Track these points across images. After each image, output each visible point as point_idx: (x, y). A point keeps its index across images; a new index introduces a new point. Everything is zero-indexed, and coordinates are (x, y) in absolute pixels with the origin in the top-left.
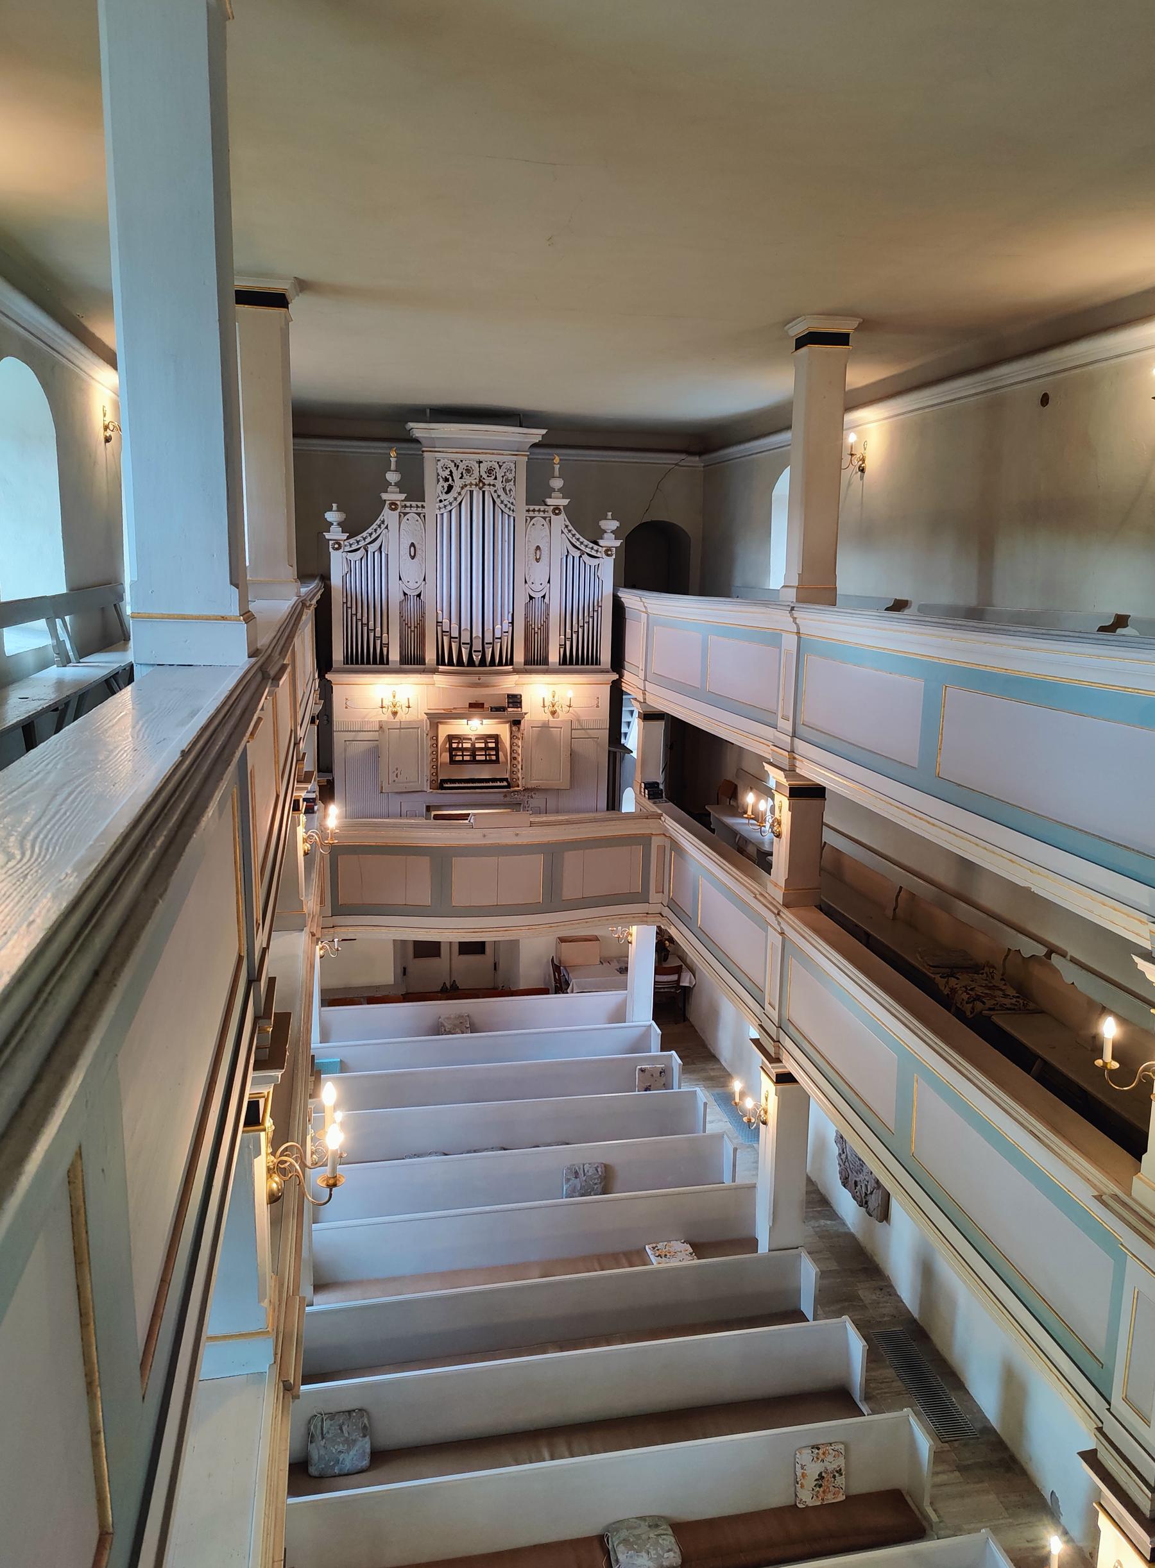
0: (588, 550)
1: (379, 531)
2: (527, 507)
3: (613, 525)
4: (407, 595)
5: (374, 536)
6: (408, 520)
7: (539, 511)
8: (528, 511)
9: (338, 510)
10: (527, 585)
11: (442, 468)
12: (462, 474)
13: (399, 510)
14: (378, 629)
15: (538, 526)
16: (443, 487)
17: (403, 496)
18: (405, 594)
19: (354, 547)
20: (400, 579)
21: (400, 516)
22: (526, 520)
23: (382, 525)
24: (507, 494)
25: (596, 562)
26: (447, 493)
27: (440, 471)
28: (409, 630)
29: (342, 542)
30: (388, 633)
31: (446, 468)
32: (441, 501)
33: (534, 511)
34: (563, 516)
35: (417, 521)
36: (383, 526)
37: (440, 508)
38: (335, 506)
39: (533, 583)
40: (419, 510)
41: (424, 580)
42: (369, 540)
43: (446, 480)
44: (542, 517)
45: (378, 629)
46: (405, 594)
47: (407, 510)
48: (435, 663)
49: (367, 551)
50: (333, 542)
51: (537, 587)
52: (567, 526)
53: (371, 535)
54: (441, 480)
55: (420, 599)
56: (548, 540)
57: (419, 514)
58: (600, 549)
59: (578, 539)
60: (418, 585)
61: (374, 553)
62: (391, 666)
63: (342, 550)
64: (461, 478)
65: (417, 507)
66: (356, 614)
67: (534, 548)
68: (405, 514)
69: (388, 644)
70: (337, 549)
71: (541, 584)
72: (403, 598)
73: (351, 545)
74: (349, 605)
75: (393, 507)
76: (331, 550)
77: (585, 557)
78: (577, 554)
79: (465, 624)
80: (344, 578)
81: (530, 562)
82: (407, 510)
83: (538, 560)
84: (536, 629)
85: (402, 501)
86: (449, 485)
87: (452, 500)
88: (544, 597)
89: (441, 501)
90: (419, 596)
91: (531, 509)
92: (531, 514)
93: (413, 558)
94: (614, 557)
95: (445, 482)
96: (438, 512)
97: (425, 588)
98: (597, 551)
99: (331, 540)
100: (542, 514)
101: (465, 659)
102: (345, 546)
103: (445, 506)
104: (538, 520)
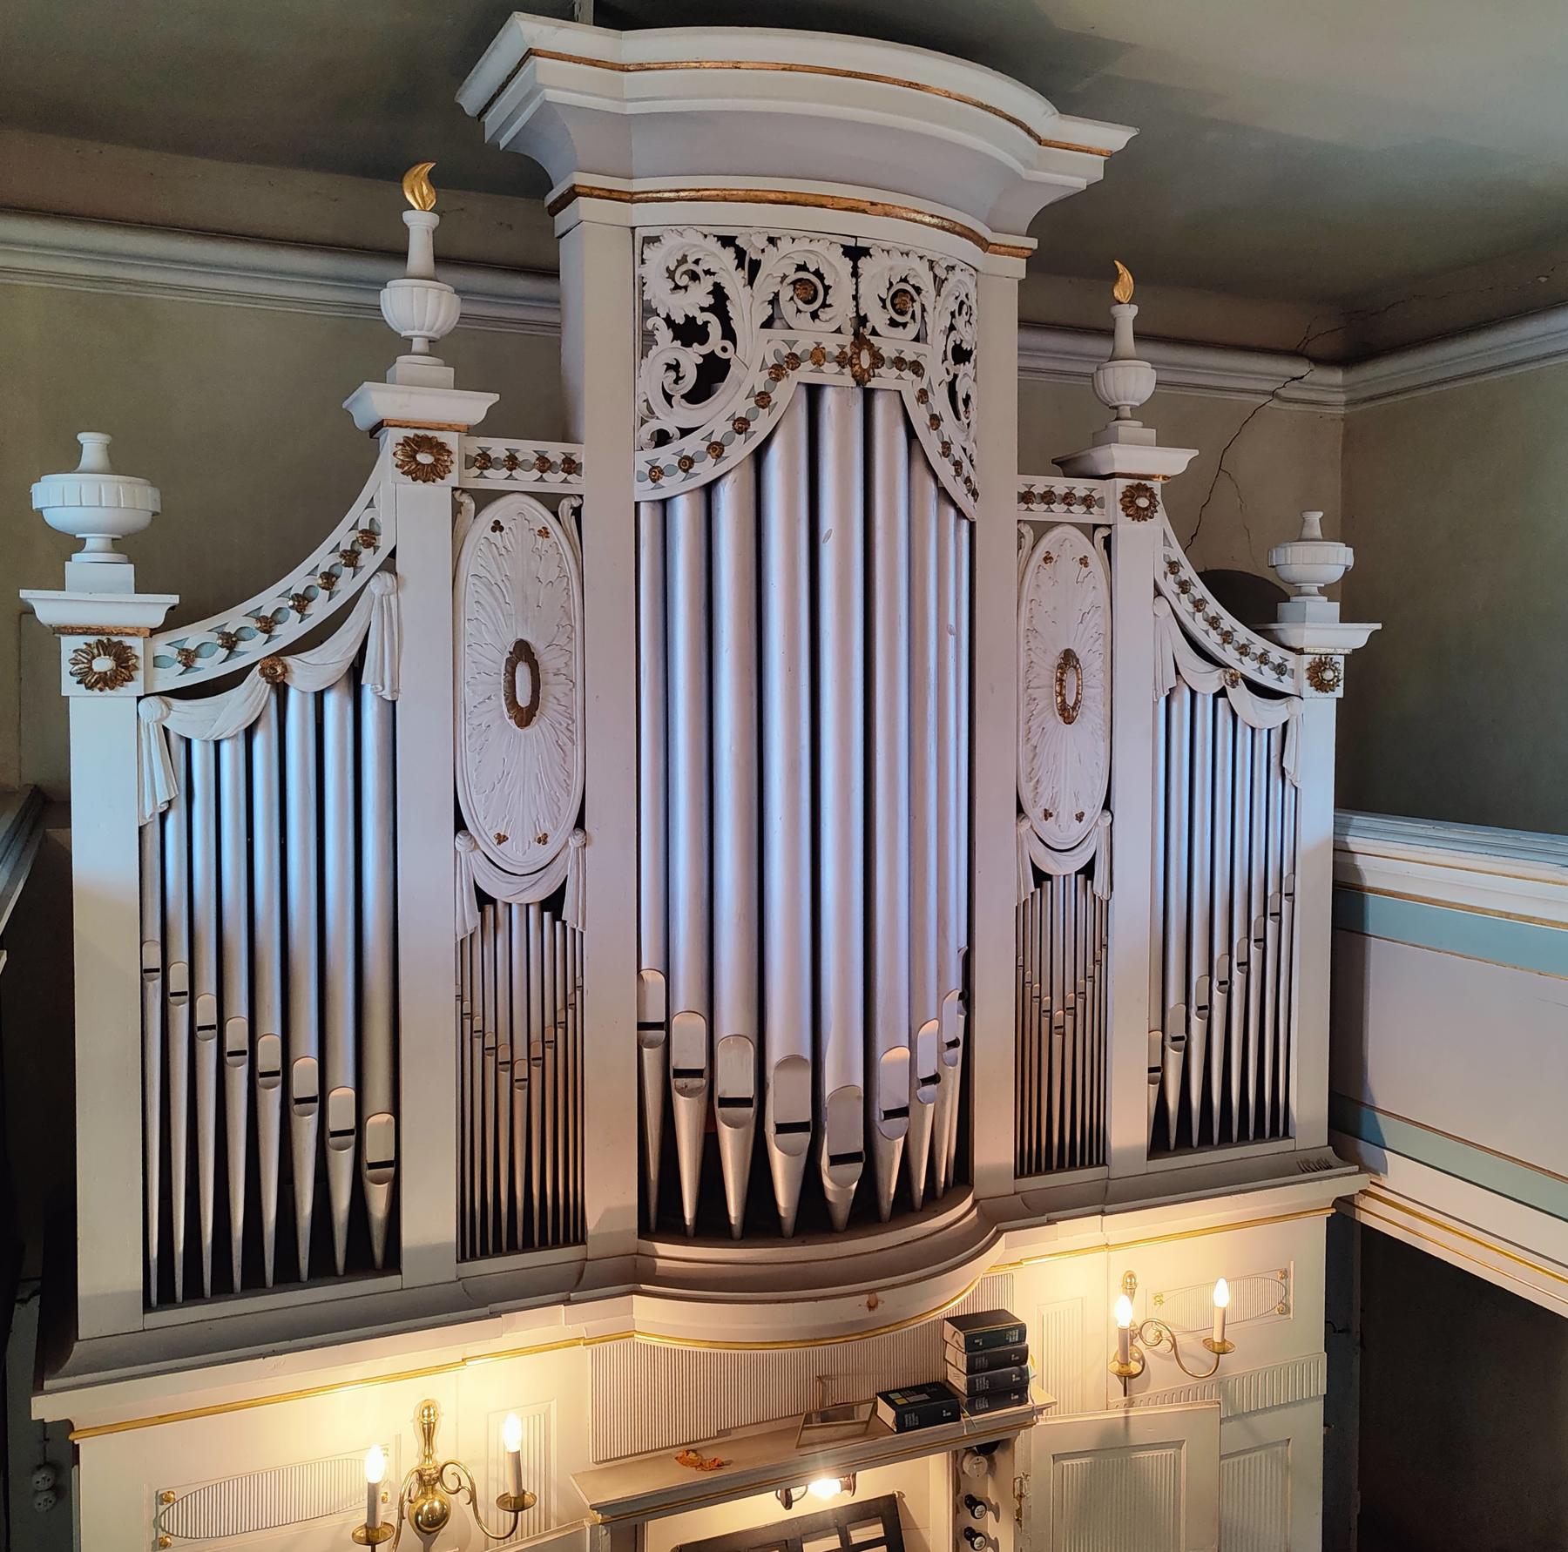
0: (1249, 668)
1: (346, 585)
2: (1021, 483)
3: (1335, 560)
4: (493, 901)
5: (321, 609)
6: (497, 527)
7: (1068, 499)
8: (1026, 498)
9: (117, 463)
10: (1026, 825)
11: (671, 274)
12: (774, 301)
13: (453, 479)
14: (342, 1096)
15: (1067, 567)
16: (674, 367)
17: (475, 406)
18: (483, 900)
19: (210, 668)
20: (460, 825)
21: (457, 508)
22: (1021, 536)
23: (366, 553)
24: (959, 419)
25: (1268, 715)
26: (698, 395)
27: (659, 292)
28: (505, 1077)
29: (136, 644)
30: (396, 1111)
31: (694, 277)
32: (662, 438)
33: (1048, 498)
34: (1160, 522)
35: (544, 533)
36: (370, 560)
37: (656, 473)
38: (92, 445)
39: (1047, 815)
40: (554, 482)
41: (580, 824)
42: (293, 628)
43: (688, 332)
44: (1080, 526)
45: (342, 1096)
46: (483, 900)
47: (496, 479)
48: (635, 1225)
49: (281, 691)
50: (79, 642)
51: (1063, 831)
52: (1173, 567)
53: (302, 602)
54: (664, 335)
55: (557, 916)
56: (1099, 620)
57: (551, 502)
58: (1292, 660)
59: (1214, 622)
60: (546, 852)
61: (319, 697)
62: (413, 1273)
63: (135, 688)
64: (768, 324)
65: (544, 464)
66: (220, 1027)
67: (1054, 658)
68: (485, 498)
69: (396, 1163)
70: (107, 681)
71: (1080, 817)
72: (472, 920)
73: (188, 659)
74: (179, 981)
75: (425, 458)
76: (69, 686)
77: (1241, 697)
78: (1208, 681)
79: (786, 1036)
80: (150, 838)
81: (1034, 724)
82: (496, 479)
83: (1068, 714)
84: (1058, 1013)
85: (471, 431)
86: (710, 358)
87: (721, 429)
88: (1088, 871)
89: (662, 438)
90: (553, 904)
91: (1035, 491)
92: (1039, 512)
93: (524, 717)
94: (1339, 692)
95: (687, 344)
96: (645, 492)
97: (581, 862)
98: (1280, 669)
99: (72, 631)
100: (1079, 513)
101: (784, 1195)
102: (157, 662)
103: (687, 463)
104: (1067, 541)
